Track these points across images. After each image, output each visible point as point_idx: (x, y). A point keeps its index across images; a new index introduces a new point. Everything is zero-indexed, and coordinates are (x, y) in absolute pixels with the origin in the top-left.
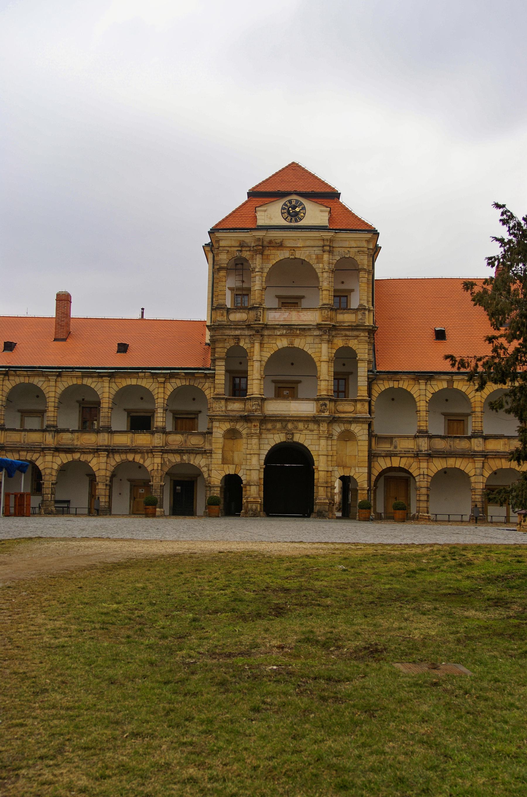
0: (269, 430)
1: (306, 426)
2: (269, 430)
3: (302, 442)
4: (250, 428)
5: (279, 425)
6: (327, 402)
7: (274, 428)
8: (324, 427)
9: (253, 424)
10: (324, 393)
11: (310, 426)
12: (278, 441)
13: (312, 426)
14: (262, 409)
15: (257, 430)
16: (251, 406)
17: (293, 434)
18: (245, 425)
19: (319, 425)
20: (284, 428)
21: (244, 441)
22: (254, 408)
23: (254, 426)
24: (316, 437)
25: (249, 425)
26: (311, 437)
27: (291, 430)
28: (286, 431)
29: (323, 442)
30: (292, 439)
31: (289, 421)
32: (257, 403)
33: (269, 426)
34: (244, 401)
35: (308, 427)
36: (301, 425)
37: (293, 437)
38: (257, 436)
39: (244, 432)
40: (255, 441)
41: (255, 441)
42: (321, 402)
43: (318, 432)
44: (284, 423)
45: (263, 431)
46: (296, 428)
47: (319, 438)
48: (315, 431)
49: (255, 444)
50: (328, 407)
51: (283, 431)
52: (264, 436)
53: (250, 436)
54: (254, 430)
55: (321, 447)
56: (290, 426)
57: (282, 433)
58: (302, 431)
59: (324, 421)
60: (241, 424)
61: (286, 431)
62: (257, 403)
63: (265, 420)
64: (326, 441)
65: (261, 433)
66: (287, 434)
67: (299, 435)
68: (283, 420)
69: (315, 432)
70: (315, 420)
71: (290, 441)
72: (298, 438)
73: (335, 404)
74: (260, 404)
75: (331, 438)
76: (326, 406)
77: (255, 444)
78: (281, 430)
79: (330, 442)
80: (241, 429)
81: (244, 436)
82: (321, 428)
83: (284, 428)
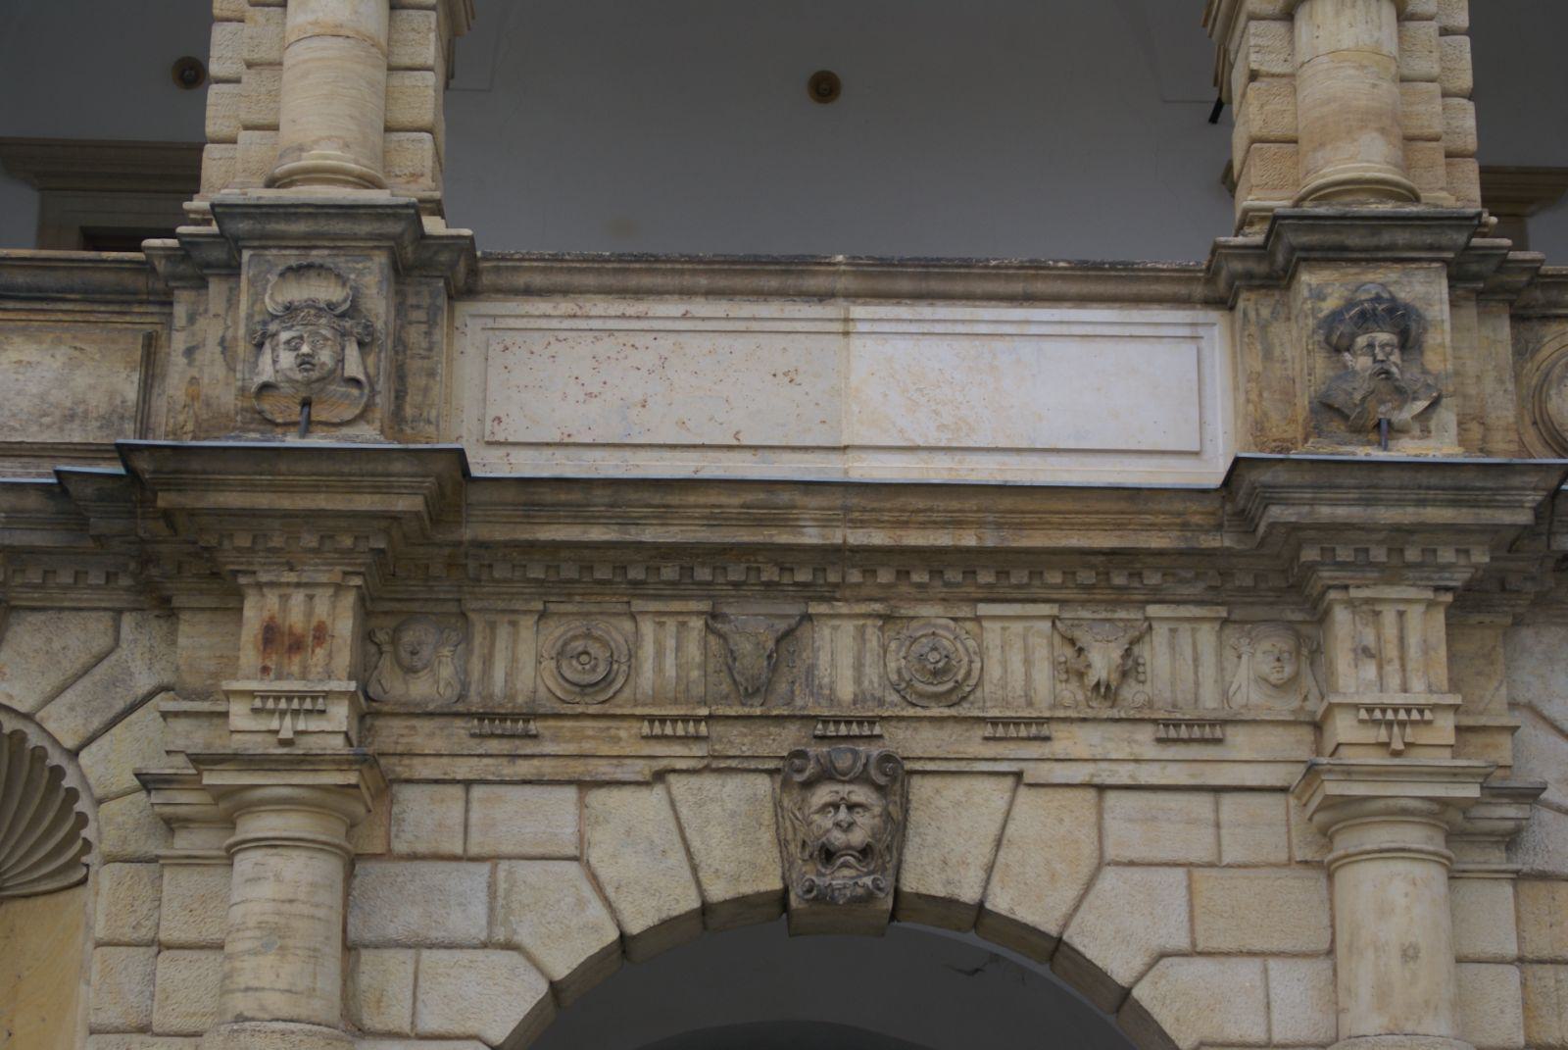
0: (505, 722)
1: (1102, 661)
2: (505, 722)
3: (1040, 913)
4: (201, 698)
5: (665, 651)
6: (1426, 290)
7: (595, 693)
8: (1389, 654)
9: (255, 612)
10: (1366, 157)
11: (1157, 655)
12: (653, 894)
13: (1192, 657)
14: (402, 386)
15: (312, 704)
16: (226, 362)
17: (893, 778)
18: (140, 658)
19: (1310, 648)
20: (757, 687)
21: (108, 898)
22: (278, 363)
23: (271, 636)
24: (1261, 829)
25: (196, 641)
26: (1182, 831)
27: (865, 723)
28: (787, 739)
29: (1395, 897)
30: (884, 850)
31: (819, 577)
32: (326, 291)
33: (520, 658)
34: (146, 319)
35: (1130, 668)
36: (1014, 653)
37: (897, 826)
38: (317, 802)
39: (107, 766)
40: (278, 882)
41: (278, 882)
42: (1325, 288)
43: (1296, 744)
44: (754, 624)
45: (425, 736)
46: (945, 689)
47: (1330, 822)
48: (1240, 742)
49: (275, 937)
50: (1434, 361)
51: (739, 741)
52: (424, 816)
53: (203, 806)
54: (264, 704)
55: (1362, 975)
56: (845, 658)
57: (715, 766)
58: (1035, 727)
59: (1395, 555)
60: (78, 636)
61: (787, 739)
62: (326, 291)
63: (448, 546)
64: (1436, 875)
65: (373, 778)
66: (794, 775)
67: (995, 794)
68: (749, 555)
69: (1255, 755)
70: (1242, 552)
71: (843, 878)
72: (980, 842)
73: (1522, 351)
74: (378, 305)
75: (1511, 840)
76: (1408, 341)
77: (275, 937)
78: (688, 736)
79: (1494, 916)
80: (64, 723)
81: (116, 822)
82: (1354, 680)
83: (756, 690)
